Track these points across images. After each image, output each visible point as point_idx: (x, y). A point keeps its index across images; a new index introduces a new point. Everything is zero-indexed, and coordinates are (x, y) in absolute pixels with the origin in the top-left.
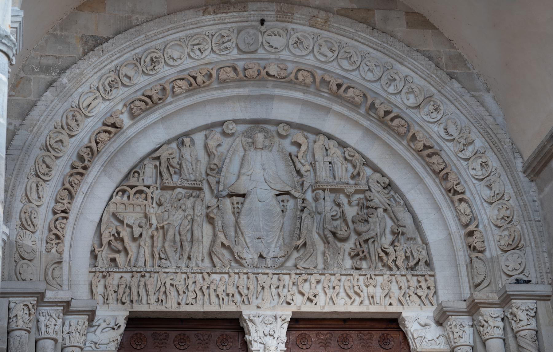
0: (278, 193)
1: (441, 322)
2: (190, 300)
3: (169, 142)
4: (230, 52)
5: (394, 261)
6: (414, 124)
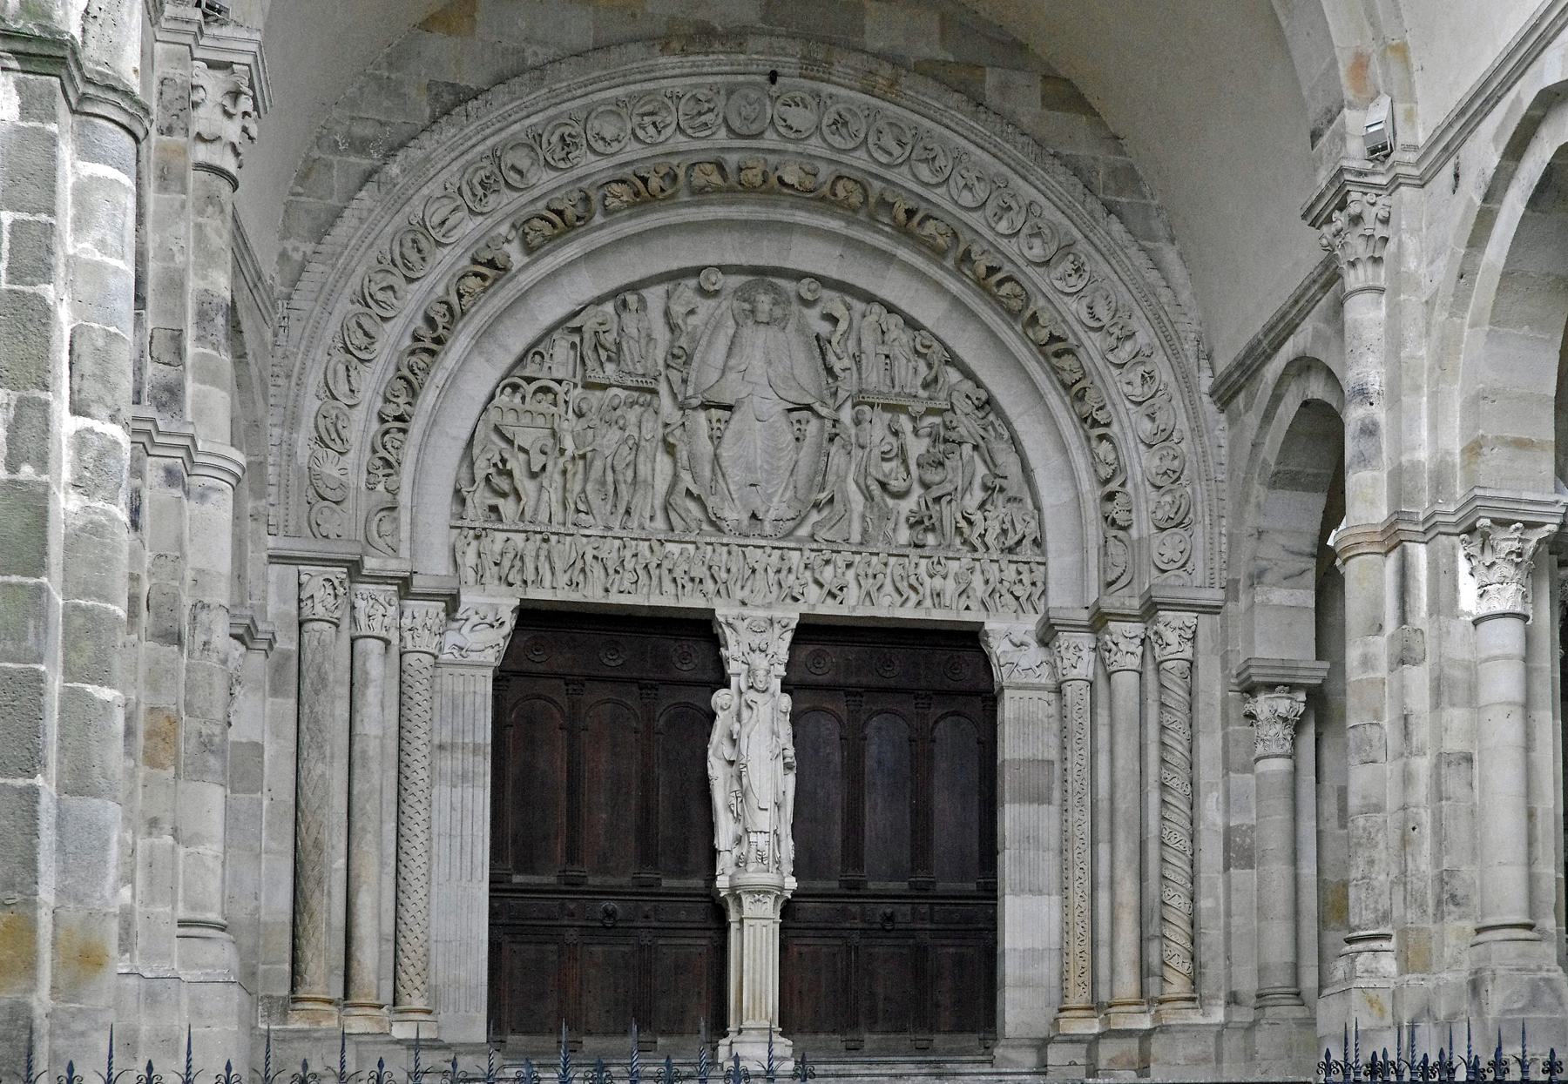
0: (791, 406)
2: (626, 585)
3: (600, 301)
5: (982, 536)
6: (1039, 296)
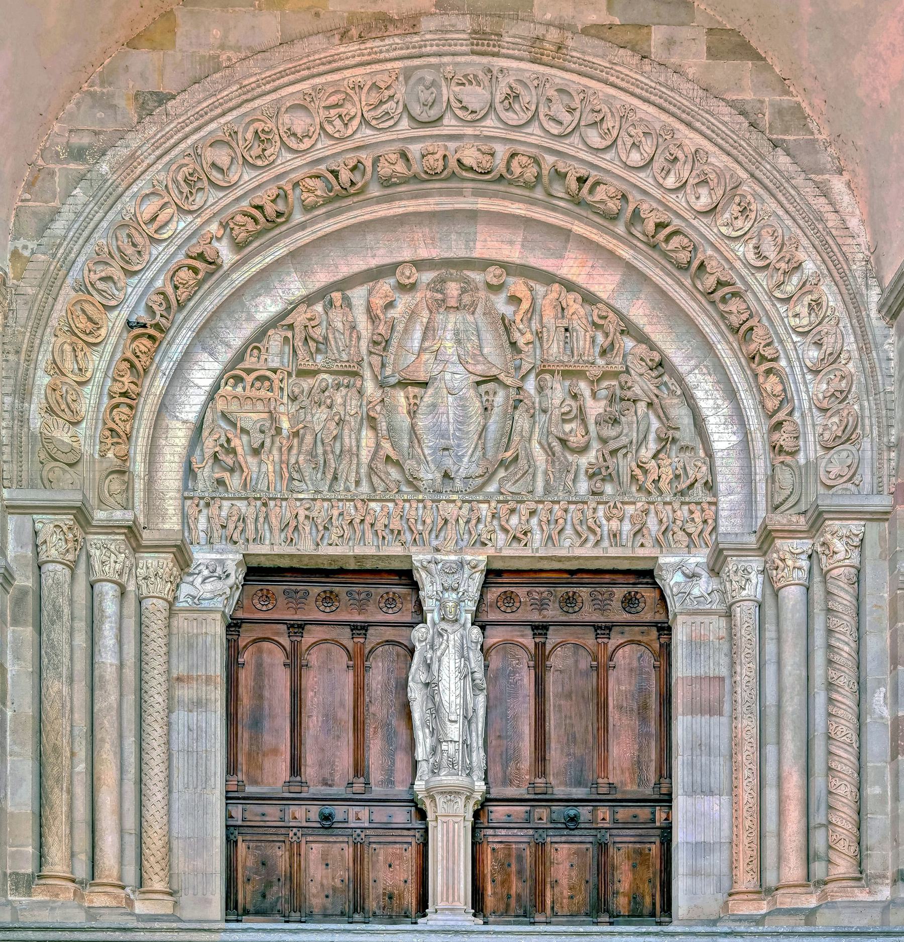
1: (716, 570)
4: (396, 124)
6: (707, 246)
